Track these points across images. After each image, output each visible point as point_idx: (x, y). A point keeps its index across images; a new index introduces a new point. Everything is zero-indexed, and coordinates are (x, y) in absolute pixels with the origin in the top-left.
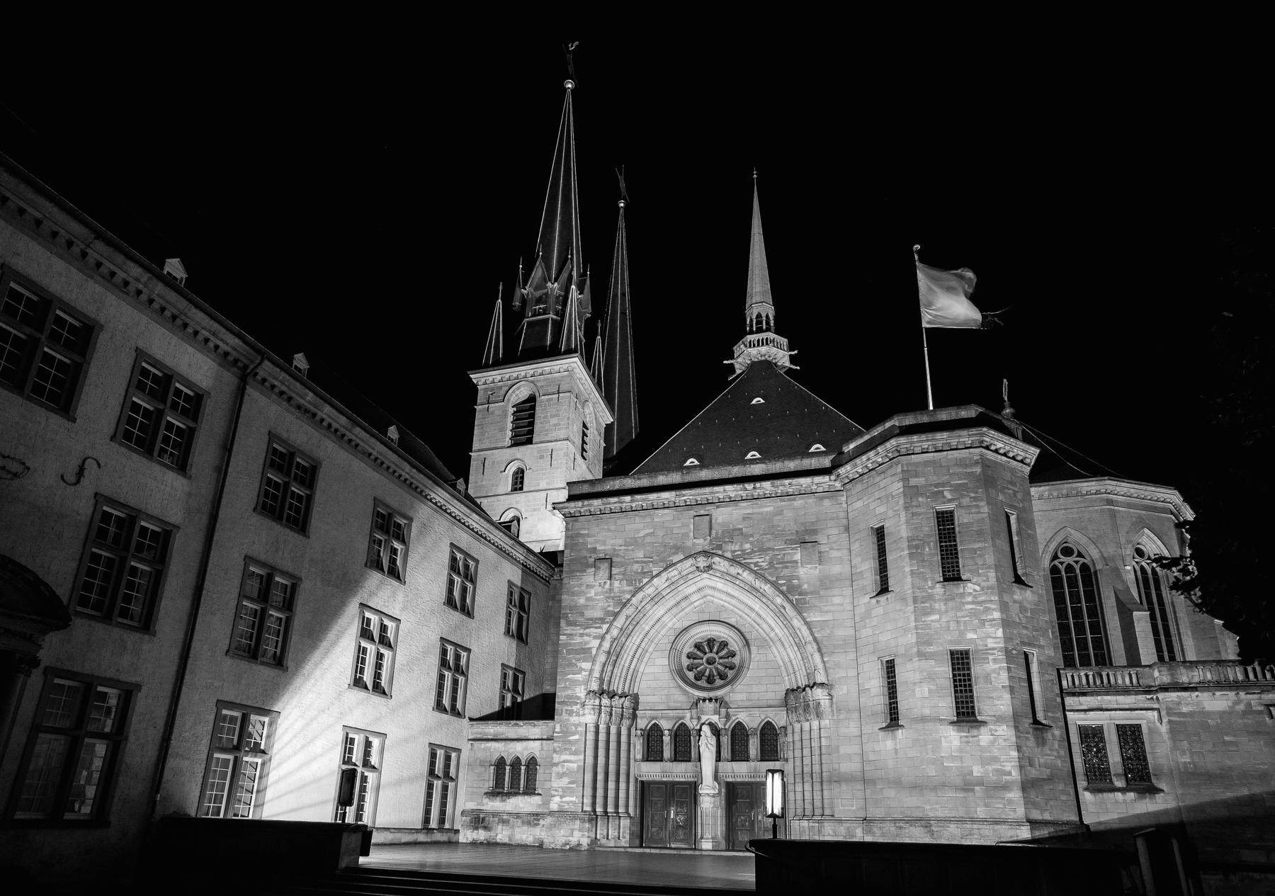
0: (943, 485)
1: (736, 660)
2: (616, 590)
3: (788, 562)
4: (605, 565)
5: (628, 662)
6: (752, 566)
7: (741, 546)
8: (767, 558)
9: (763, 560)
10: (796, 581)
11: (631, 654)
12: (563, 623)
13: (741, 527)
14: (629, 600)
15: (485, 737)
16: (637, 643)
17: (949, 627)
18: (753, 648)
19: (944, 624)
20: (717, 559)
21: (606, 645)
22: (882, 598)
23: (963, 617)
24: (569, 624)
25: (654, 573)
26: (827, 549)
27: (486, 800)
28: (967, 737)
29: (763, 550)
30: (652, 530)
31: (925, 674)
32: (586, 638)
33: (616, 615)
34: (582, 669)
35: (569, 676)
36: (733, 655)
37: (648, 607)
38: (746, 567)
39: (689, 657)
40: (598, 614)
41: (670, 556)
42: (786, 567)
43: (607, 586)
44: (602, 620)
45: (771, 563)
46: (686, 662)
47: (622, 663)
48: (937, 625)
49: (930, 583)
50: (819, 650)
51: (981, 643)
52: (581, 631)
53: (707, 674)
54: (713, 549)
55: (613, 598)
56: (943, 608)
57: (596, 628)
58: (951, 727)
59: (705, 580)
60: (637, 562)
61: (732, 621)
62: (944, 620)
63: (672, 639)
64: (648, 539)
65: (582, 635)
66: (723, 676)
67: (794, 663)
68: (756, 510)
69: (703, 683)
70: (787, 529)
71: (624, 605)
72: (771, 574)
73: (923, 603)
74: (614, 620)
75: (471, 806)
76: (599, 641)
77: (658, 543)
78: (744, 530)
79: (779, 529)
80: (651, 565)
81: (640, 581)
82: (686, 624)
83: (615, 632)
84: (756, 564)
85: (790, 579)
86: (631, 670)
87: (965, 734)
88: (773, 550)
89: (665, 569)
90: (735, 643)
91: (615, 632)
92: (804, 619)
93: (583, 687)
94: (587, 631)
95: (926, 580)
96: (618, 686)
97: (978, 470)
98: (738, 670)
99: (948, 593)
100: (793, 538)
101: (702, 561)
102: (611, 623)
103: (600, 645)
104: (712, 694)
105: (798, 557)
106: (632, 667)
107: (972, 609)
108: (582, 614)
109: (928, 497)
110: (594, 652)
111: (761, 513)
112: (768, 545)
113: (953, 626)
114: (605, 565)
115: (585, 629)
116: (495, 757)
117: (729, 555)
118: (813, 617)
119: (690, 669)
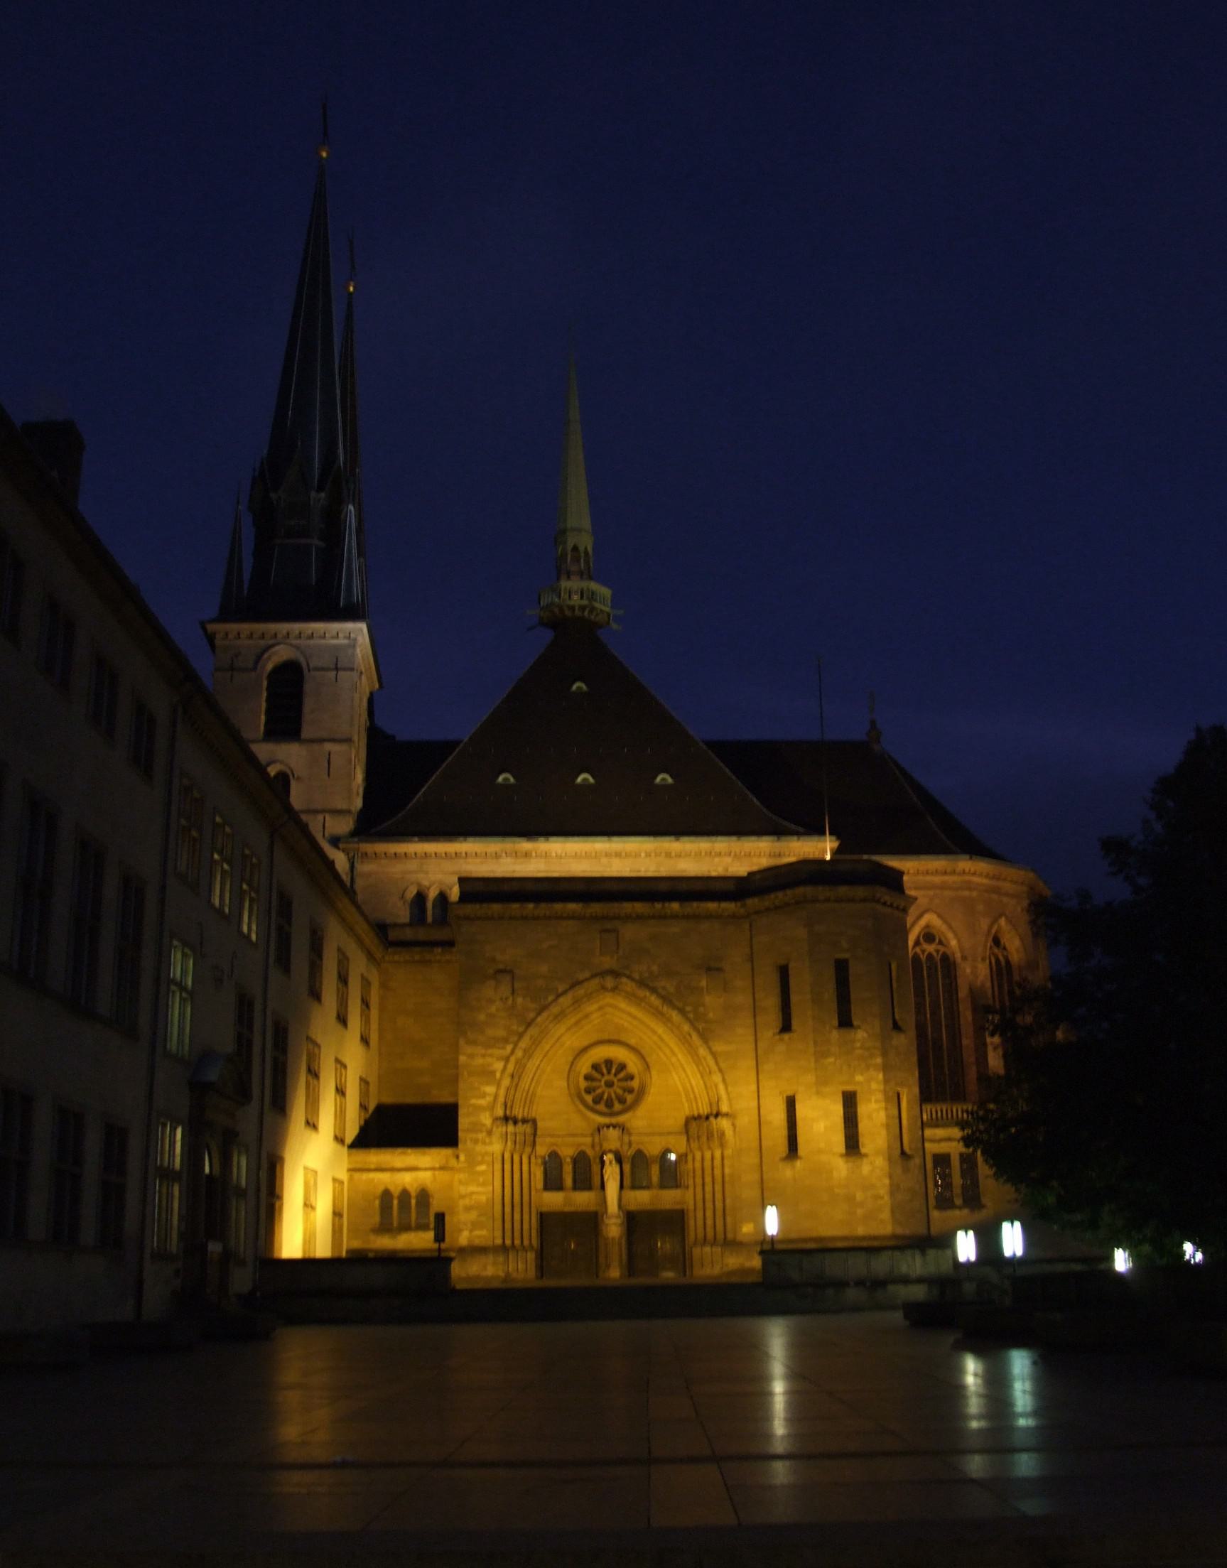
1: (635, 1084)
5: (528, 1083)
6: (660, 990)
11: (531, 1077)
12: (462, 1042)
15: (367, 1166)
18: (654, 1072)
20: (624, 980)
21: (511, 1067)
22: (786, 1036)
25: (560, 990)
27: (372, 1237)
32: (489, 1060)
33: (521, 1036)
35: (473, 1101)
36: (631, 1078)
38: (653, 990)
43: (510, 1001)
46: (583, 1084)
50: (724, 1080)
53: (605, 1097)
59: (608, 999)
61: (633, 1042)
63: (571, 1059)
65: (484, 1056)
66: (622, 1101)
67: (696, 1091)
69: (601, 1107)
82: (586, 1043)
89: (573, 986)
90: (633, 1066)
91: (519, 1053)
92: (710, 1048)
94: (490, 1051)
96: (518, 1112)
98: (641, 1093)
101: (609, 982)
102: (516, 1045)
104: (614, 1120)
105: (704, 983)
106: (532, 1089)
110: (498, 1075)
116: (380, 1189)
119: (588, 1091)
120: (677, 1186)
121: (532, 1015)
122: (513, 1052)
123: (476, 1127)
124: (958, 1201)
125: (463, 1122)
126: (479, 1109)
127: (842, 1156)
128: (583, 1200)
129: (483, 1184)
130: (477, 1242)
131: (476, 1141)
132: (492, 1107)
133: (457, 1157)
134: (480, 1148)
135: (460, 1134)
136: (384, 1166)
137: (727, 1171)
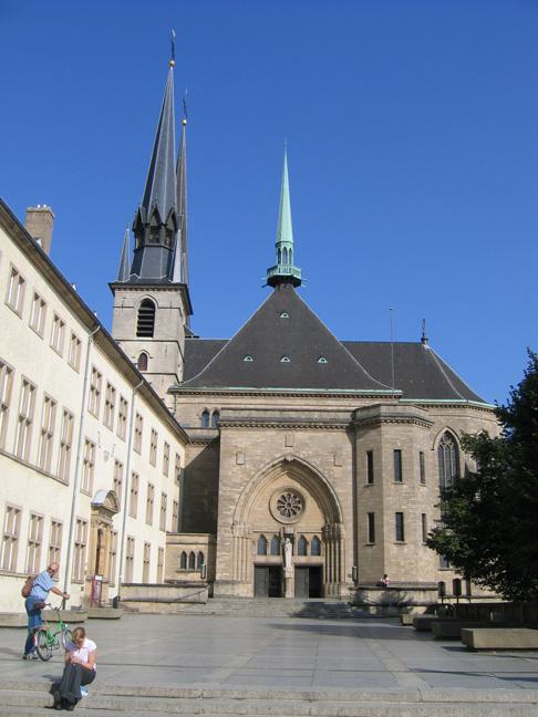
4: (242, 456)
21: (242, 497)
24: (224, 485)
25: (267, 460)
33: (248, 482)
40: (239, 481)
44: (241, 485)
45: (321, 463)
75: (169, 578)
83: (247, 490)
85: (330, 470)
114: (242, 456)
117: (302, 456)
118: (338, 490)
120: (319, 554)
123: (226, 525)
125: (220, 522)
126: (228, 516)
128: (276, 560)
130: (224, 579)
131: (225, 531)
133: (216, 537)
134: (227, 535)
135: (219, 528)
137: (342, 549)
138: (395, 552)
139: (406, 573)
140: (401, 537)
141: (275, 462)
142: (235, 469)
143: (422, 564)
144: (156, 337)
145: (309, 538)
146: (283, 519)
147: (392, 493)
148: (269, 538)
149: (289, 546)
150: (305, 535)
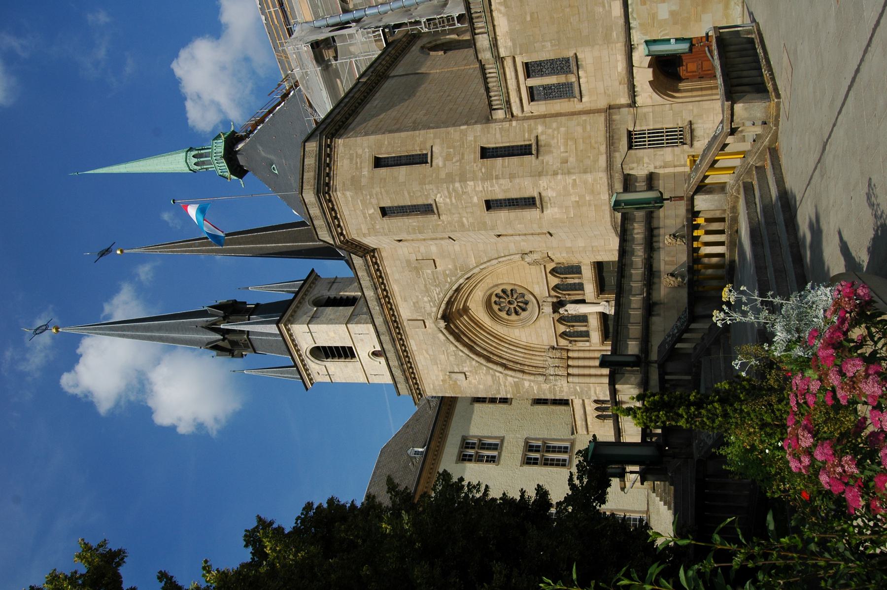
0: (364, 214)
2: (470, 369)
3: (434, 276)
7: (426, 302)
8: (432, 288)
9: (434, 291)
10: (447, 272)
13: (412, 303)
14: (476, 361)
15: (584, 426)
16: (506, 350)
17: (471, 212)
19: (469, 215)
23: (462, 204)
25: (453, 348)
26: (420, 254)
28: (550, 204)
29: (427, 290)
30: (424, 351)
31: (508, 226)
32: (507, 384)
34: (529, 386)
35: (535, 391)
37: (478, 349)
39: (512, 290)
40: (489, 378)
41: (441, 341)
42: (438, 278)
45: (436, 286)
47: (522, 359)
48: (471, 220)
49: (439, 223)
51: (480, 194)
52: (503, 387)
54: (431, 318)
55: (476, 371)
56: (457, 215)
57: (499, 379)
58: (545, 212)
60: (448, 359)
62: (466, 215)
64: (431, 352)
65: (505, 386)
68: (398, 294)
70: (409, 277)
71: (481, 364)
72: (445, 286)
73: (455, 227)
74: (492, 369)
76: (508, 377)
77: (432, 348)
78: (414, 301)
79: (409, 281)
80: (449, 351)
81: (462, 356)
84: (438, 294)
86: (526, 351)
87: (549, 205)
88: (425, 286)
92: (475, 268)
93: (542, 385)
94: (502, 383)
95: (439, 225)
97: (348, 194)
99: (445, 213)
100: (415, 273)
102: (496, 371)
103: (511, 376)
107: (455, 199)
108: (490, 386)
109: (375, 223)
111: (400, 292)
112: (423, 288)
113: (469, 210)
115: (501, 385)
117: (434, 309)
118: (472, 262)
121: (474, 363)
122: (501, 373)
124: (572, 78)
126: (539, 388)
127: (543, 212)
128: (594, 323)
129: (589, 389)
132: (538, 384)
136: (583, 417)
138: (556, 210)
139: (592, 192)
140: (529, 203)
141: (451, 338)
142: (473, 381)
143: (572, 160)
144: (350, 344)
145: (554, 281)
146: (533, 307)
147: (456, 217)
148: (562, 328)
149: (572, 309)
150: (552, 285)
